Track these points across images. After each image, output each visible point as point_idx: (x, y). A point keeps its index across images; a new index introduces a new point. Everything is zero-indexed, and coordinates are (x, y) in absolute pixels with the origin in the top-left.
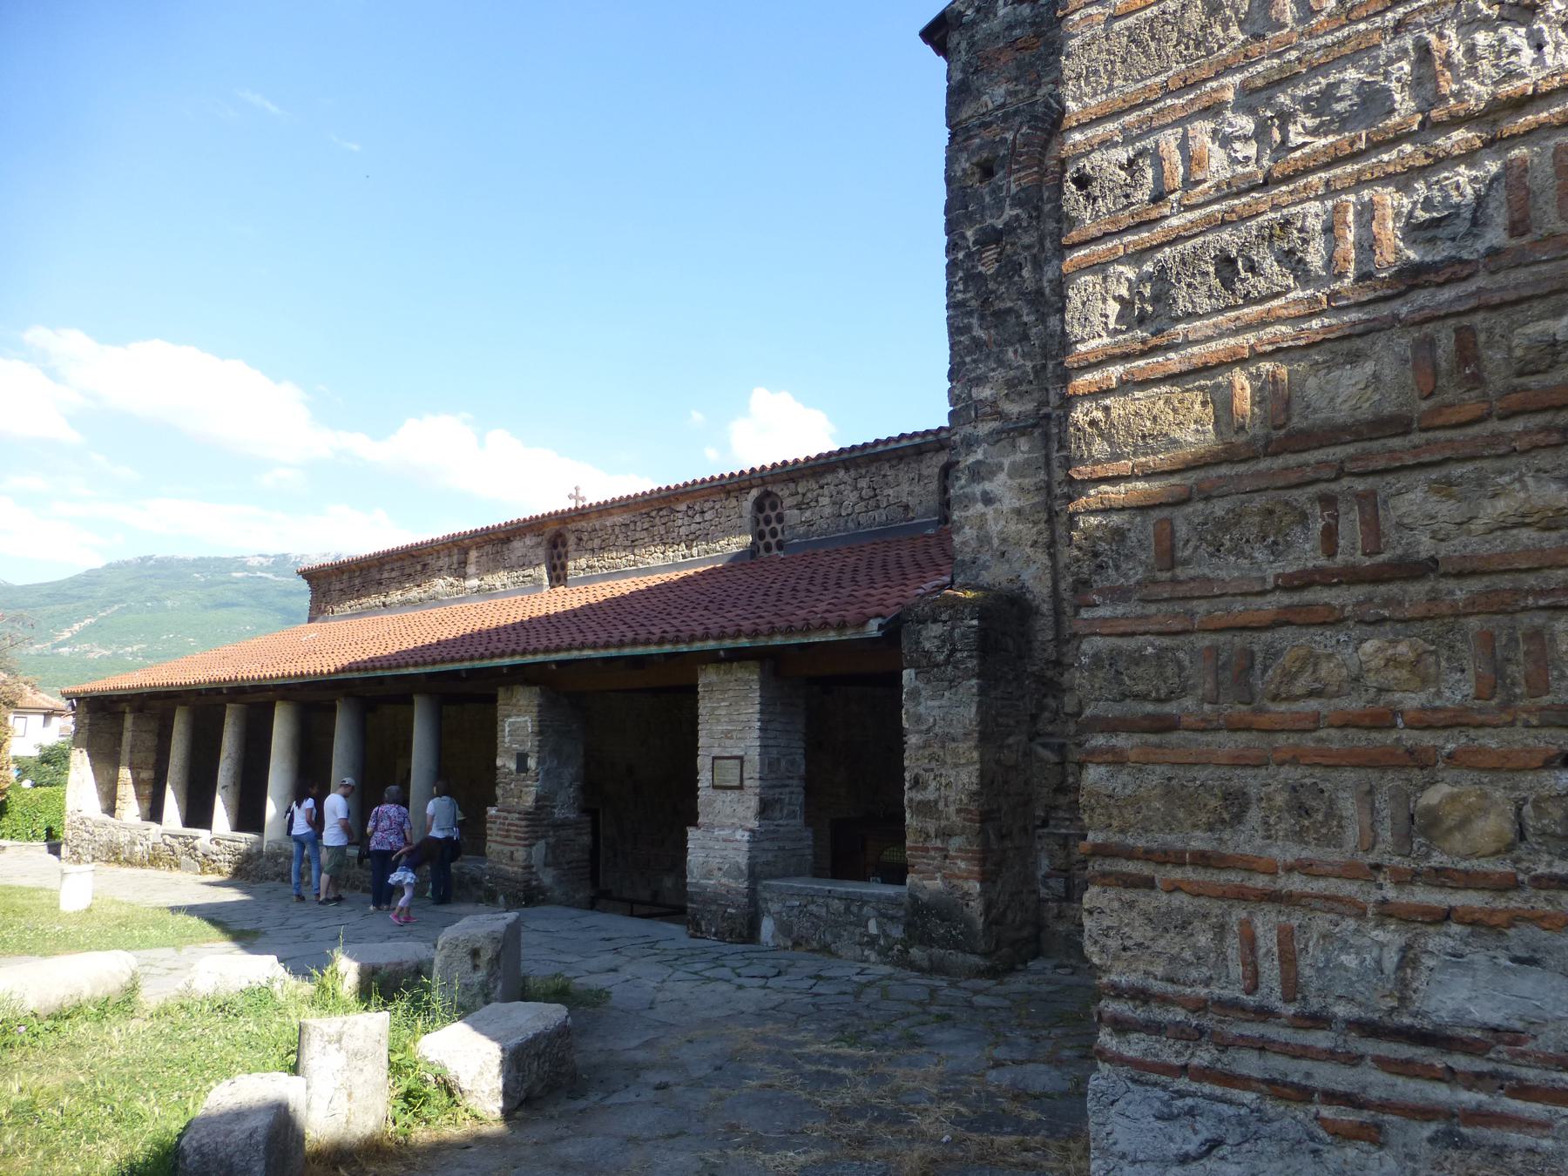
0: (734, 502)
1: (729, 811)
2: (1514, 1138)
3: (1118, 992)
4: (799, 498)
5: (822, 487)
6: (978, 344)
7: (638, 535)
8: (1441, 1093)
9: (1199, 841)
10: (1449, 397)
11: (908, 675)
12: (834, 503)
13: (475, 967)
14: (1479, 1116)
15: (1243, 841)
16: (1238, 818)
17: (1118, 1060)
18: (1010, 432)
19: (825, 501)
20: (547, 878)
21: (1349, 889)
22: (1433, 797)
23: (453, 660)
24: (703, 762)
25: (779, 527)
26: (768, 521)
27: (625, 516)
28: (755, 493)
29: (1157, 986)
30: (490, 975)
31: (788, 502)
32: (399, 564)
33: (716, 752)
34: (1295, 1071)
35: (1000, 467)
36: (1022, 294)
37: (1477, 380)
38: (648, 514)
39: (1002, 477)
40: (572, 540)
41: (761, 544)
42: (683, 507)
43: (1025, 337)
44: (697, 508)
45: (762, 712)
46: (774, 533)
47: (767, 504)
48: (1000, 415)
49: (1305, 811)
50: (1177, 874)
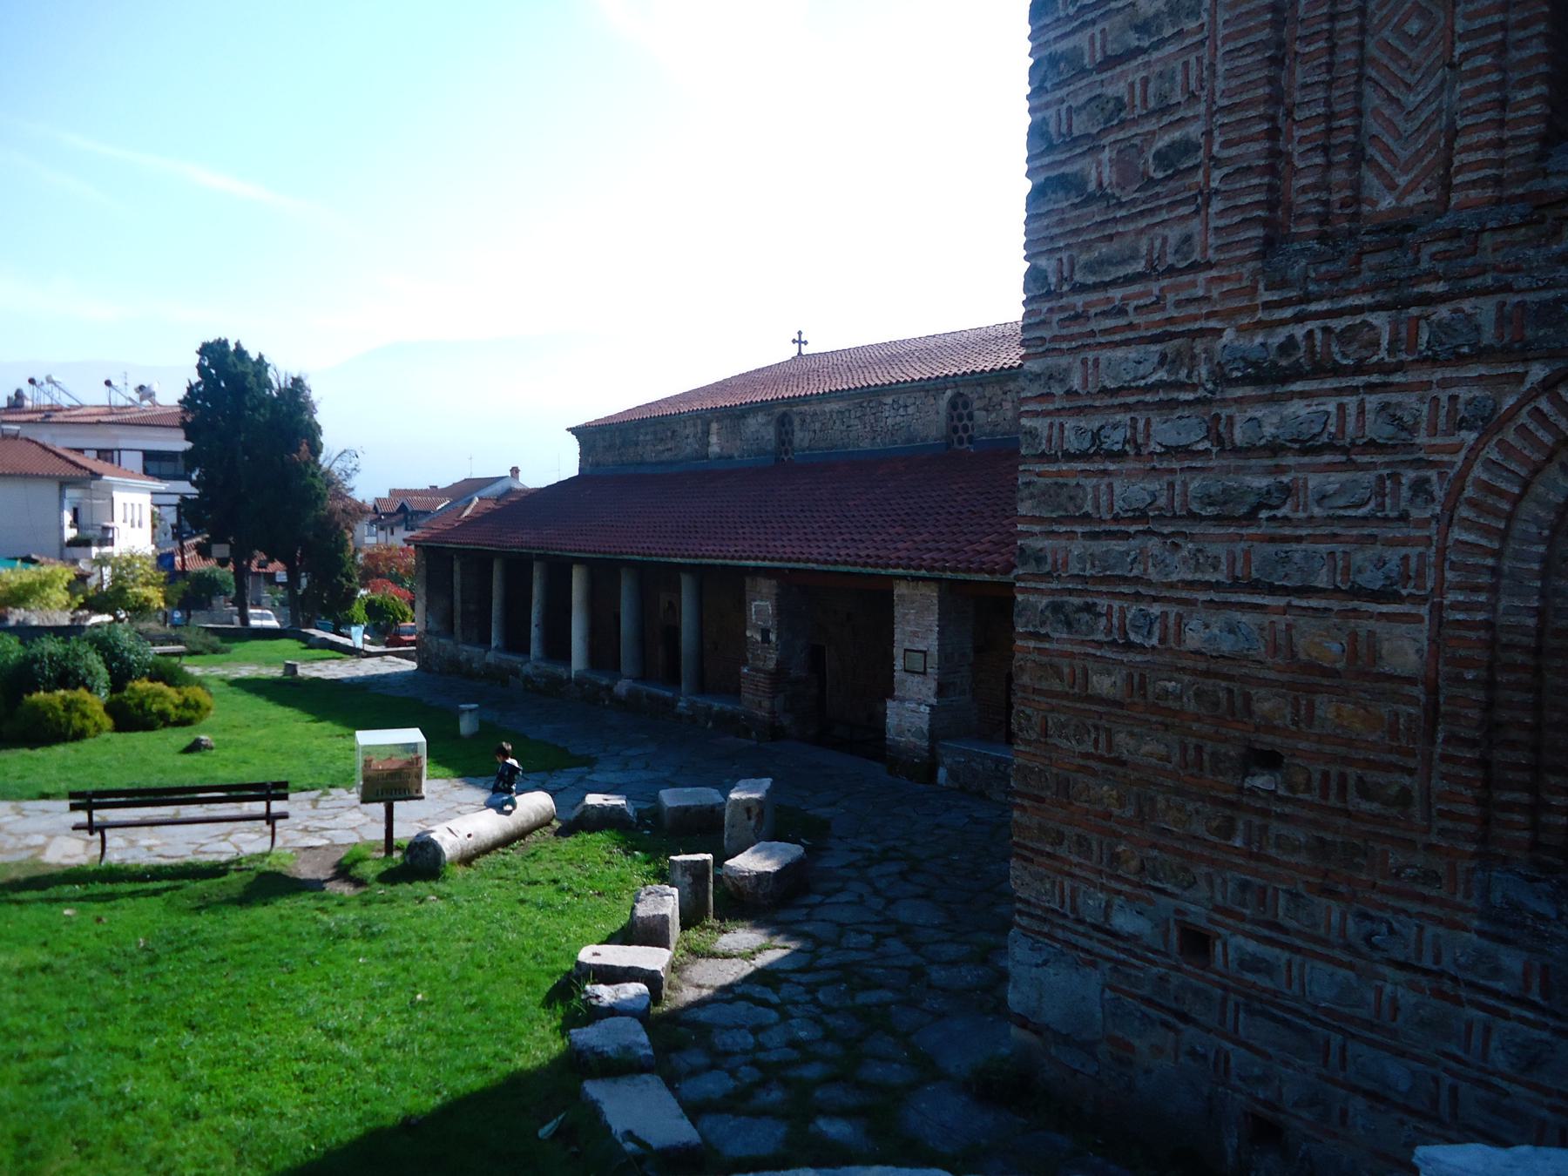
0: (933, 401)
1: (916, 689)
2: (1133, 972)
3: (1020, 900)
5: (1005, 393)
7: (852, 422)
8: (1114, 954)
9: (1048, 849)
10: (1136, 700)
13: (749, 818)
14: (1124, 963)
15: (1062, 851)
16: (1061, 843)
17: (1019, 926)
19: (1008, 405)
20: (786, 721)
21: (1092, 876)
22: (1121, 848)
23: (710, 557)
24: (898, 652)
25: (970, 424)
26: (960, 418)
27: (841, 404)
28: (949, 393)
29: (1033, 900)
30: (757, 822)
31: (977, 404)
32: (652, 429)
33: (907, 645)
34: (1073, 938)
37: (1145, 696)
40: (797, 422)
42: (889, 400)
45: (939, 620)
46: (965, 429)
47: (960, 401)
49: (1081, 845)
50: (1042, 859)
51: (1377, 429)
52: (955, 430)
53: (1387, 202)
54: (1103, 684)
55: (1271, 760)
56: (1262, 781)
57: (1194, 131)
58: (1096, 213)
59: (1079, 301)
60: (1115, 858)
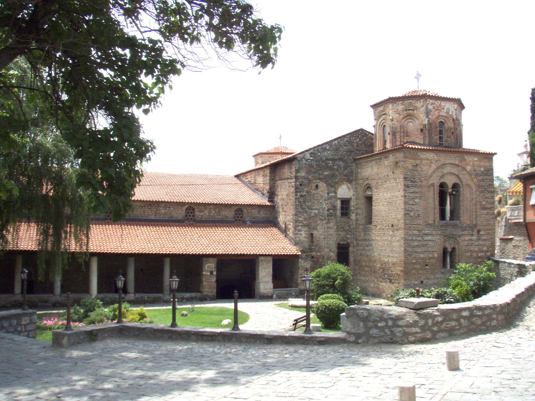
0: (180, 207)
4: (199, 210)
5: (206, 208)
6: (300, 212)
11: (300, 260)
12: (209, 213)
18: (304, 226)
19: (207, 211)
26: (188, 213)
28: (187, 206)
31: (196, 210)
35: (303, 230)
36: (306, 206)
38: (150, 205)
39: (303, 232)
41: (186, 218)
43: (307, 213)
44: (168, 206)
46: (190, 216)
48: (302, 223)
51: (434, 239)
52: (186, 216)
53: (430, 222)
54: (414, 261)
55: (426, 265)
56: (427, 267)
57: (420, 213)
58: (412, 218)
59: (410, 226)
60: (415, 277)
